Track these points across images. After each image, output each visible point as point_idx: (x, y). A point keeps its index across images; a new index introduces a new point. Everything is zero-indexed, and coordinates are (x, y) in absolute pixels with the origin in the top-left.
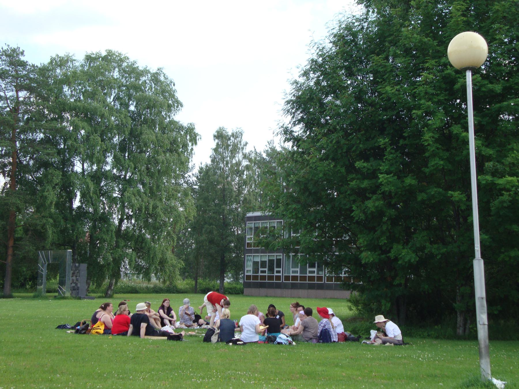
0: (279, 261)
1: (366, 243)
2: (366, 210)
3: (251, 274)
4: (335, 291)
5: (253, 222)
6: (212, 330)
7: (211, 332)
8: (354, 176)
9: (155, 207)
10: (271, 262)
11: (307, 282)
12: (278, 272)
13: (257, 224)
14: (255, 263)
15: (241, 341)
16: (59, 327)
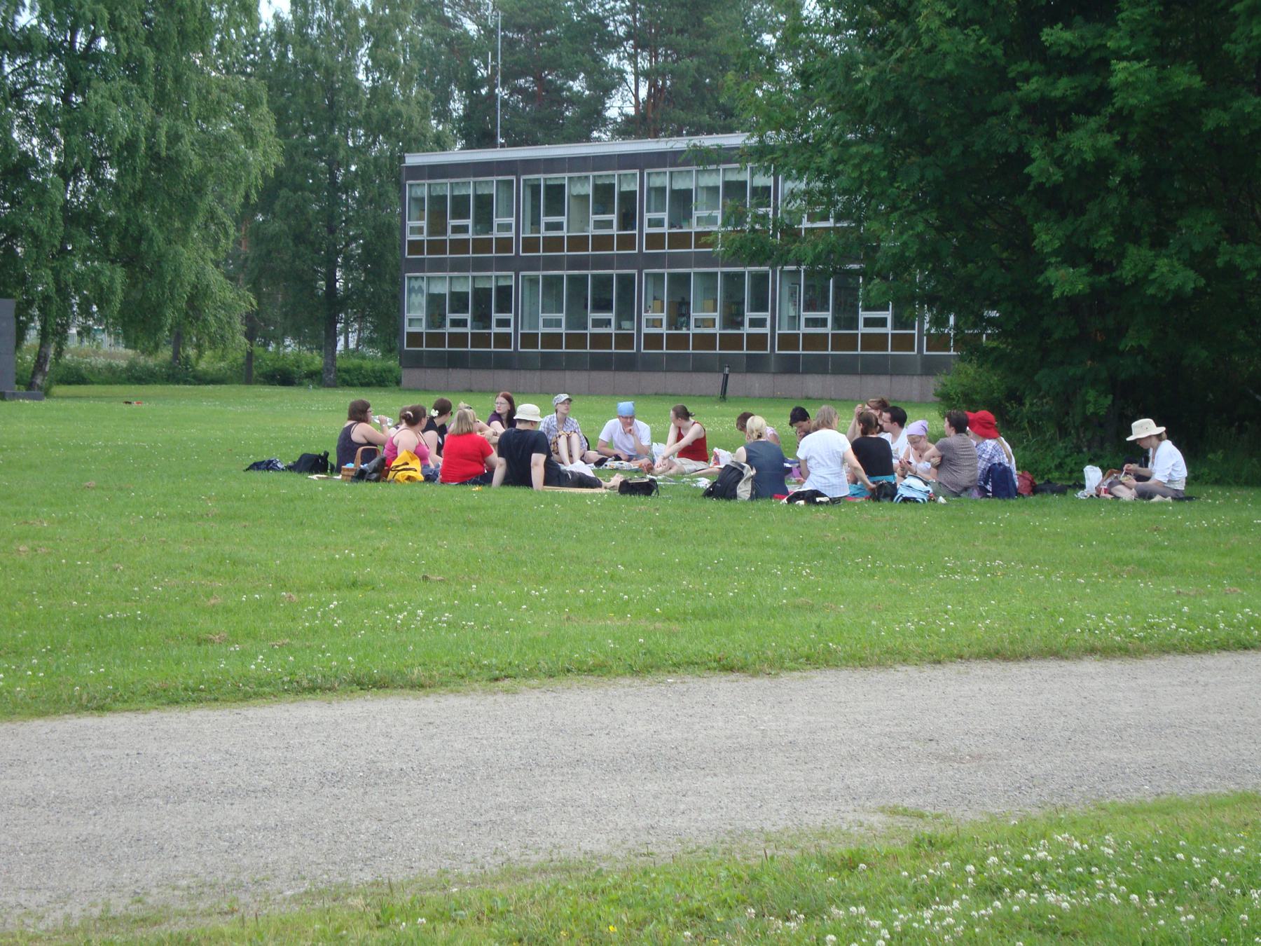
0: (504, 292)
1: (1057, 244)
2: (1067, 158)
3: (422, 328)
4: (670, 376)
5: (427, 182)
6: (734, 469)
7: (734, 474)
8: (1026, 65)
9: (175, 138)
10: (482, 296)
11: (588, 350)
12: (502, 323)
13: (438, 188)
14: (435, 301)
15: (823, 495)
16: (256, 466)
